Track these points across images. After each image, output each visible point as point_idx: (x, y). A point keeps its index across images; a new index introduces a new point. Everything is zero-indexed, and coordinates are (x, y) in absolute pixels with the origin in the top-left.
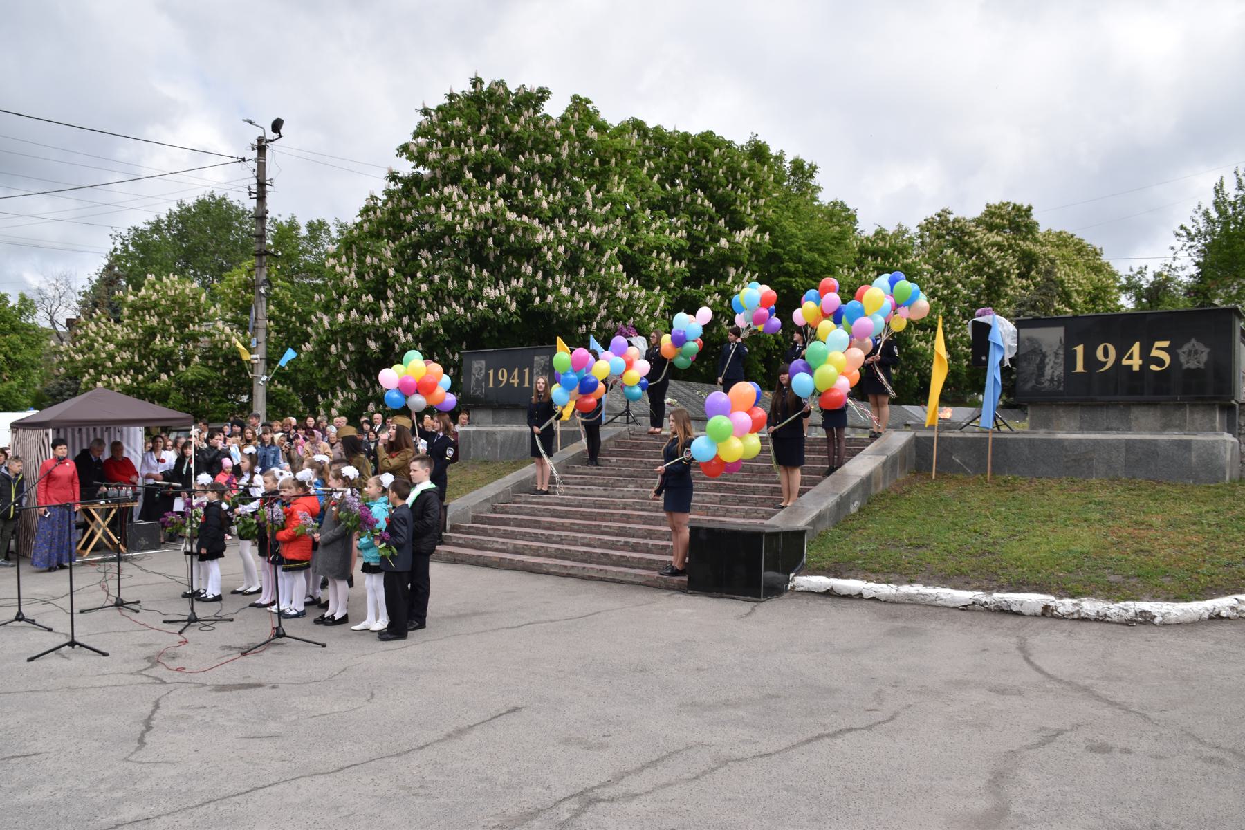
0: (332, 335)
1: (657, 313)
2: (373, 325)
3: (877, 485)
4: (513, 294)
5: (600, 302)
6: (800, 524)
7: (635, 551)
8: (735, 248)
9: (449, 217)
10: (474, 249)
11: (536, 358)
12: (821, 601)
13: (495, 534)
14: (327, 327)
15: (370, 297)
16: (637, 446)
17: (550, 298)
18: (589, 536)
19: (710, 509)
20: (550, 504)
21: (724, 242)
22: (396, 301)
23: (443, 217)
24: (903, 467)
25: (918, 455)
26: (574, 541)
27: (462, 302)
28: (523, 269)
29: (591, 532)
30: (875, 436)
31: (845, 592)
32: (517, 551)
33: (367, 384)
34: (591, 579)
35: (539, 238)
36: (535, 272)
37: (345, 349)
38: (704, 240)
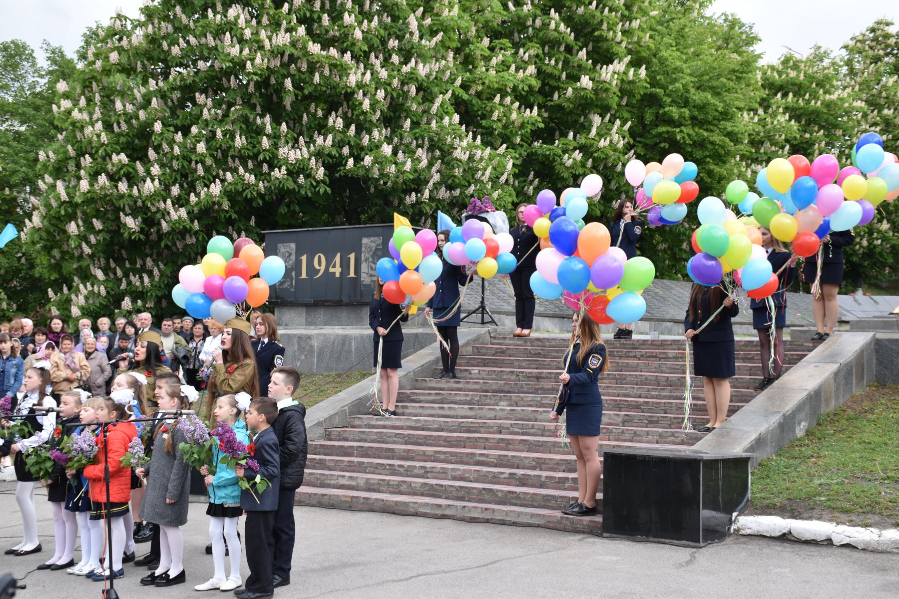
0: (71, 209)
1: (503, 179)
2: (130, 196)
3: (827, 401)
4: (318, 154)
5: (431, 165)
6: (737, 450)
7: (524, 485)
8: (600, 88)
9: (235, 51)
10: (267, 94)
11: (365, 241)
12: (778, 547)
13: (336, 466)
14: (64, 197)
15: (123, 157)
16: (503, 352)
17: (368, 160)
18: (462, 467)
19: (626, 433)
20: (401, 428)
21: (585, 81)
22: (162, 166)
23: (228, 50)
24: (860, 378)
25: (880, 363)
26: (443, 474)
27: (250, 164)
28: (331, 121)
29: (462, 463)
30: (821, 338)
31: (808, 536)
32: (370, 487)
33: (119, 273)
34: (473, 520)
35: (353, 80)
36: (347, 126)
37: (90, 227)
38: (560, 77)
